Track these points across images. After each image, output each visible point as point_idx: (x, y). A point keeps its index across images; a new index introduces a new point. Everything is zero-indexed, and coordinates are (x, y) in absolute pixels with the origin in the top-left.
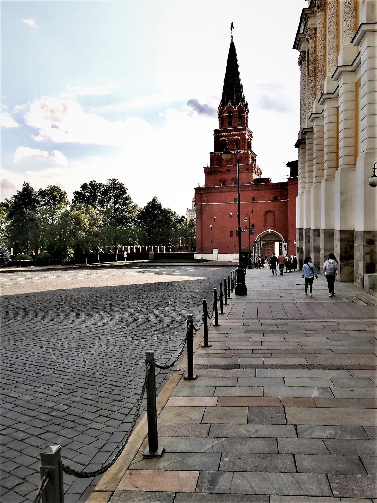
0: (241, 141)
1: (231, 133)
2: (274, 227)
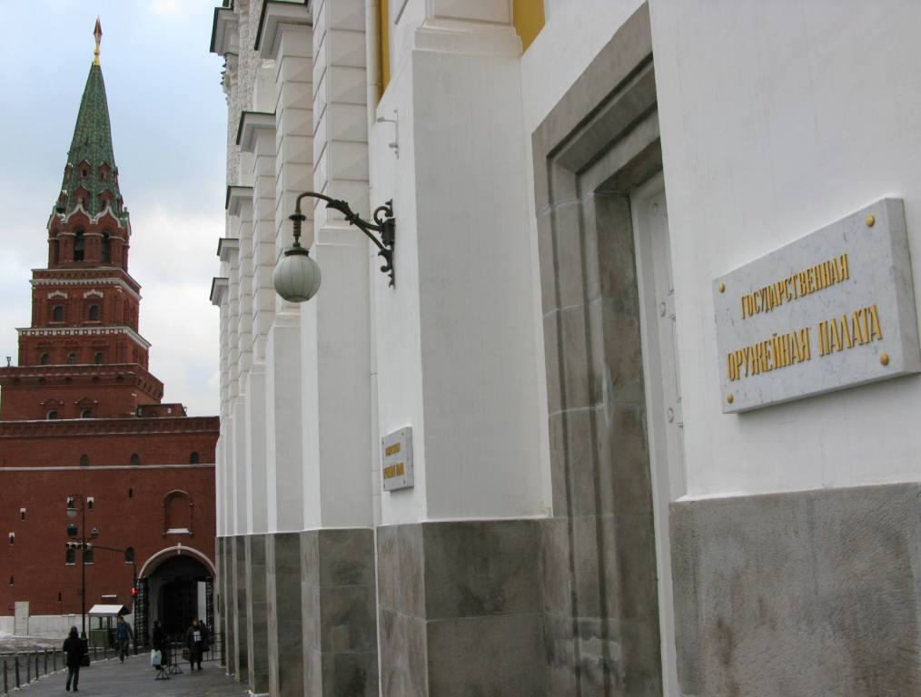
1: (81, 281)
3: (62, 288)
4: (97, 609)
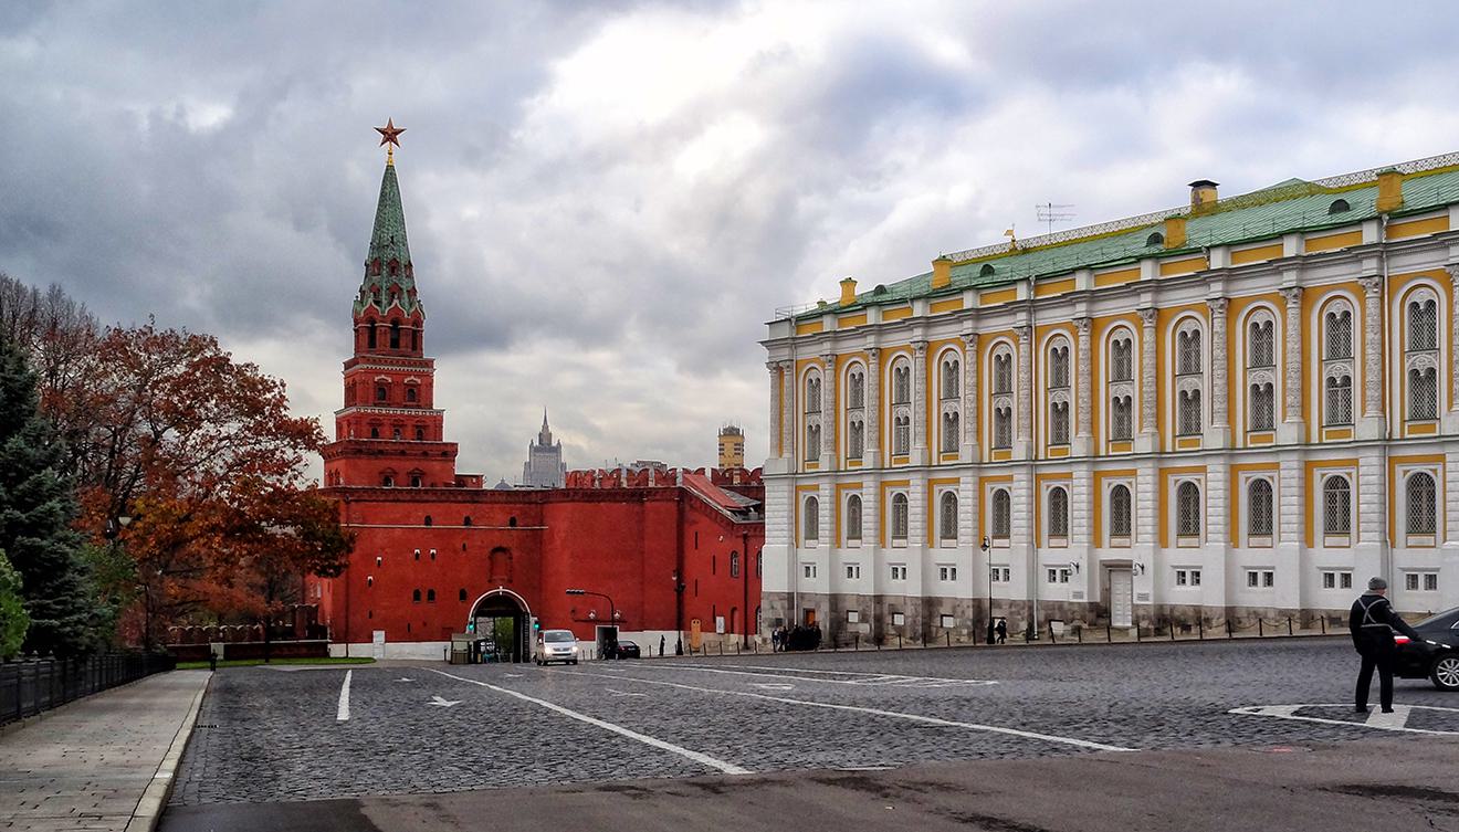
0: (423, 388)
2: (509, 583)
3: (387, 373)
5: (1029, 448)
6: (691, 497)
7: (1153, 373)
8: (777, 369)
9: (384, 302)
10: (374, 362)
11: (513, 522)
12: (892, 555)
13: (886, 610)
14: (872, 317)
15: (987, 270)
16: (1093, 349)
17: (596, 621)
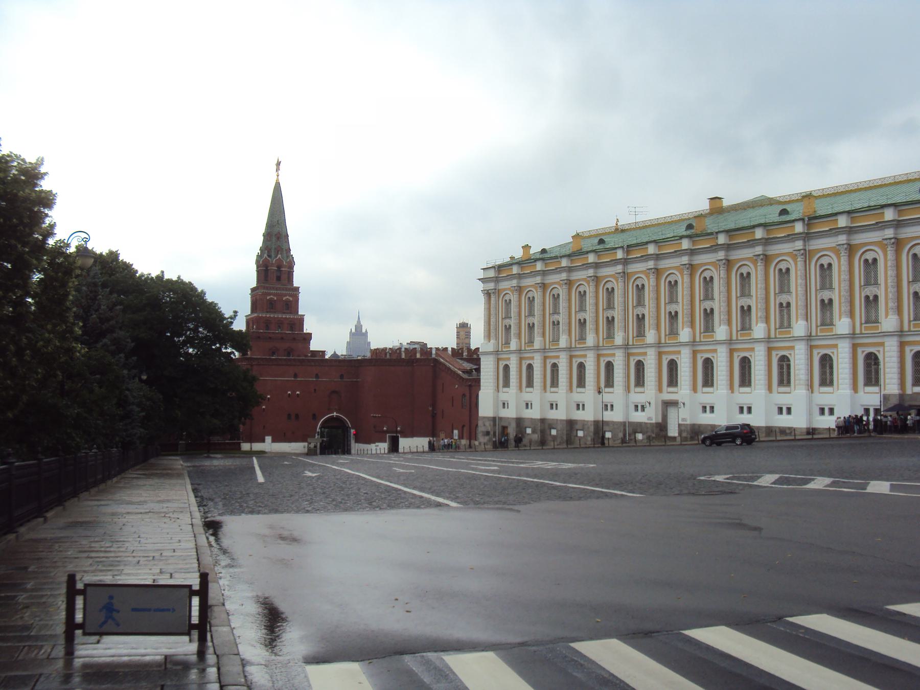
3: (274, 295)
4: (309, 440)
5: (624, 339)
6: (441, 363)
7: (689, 298)
8: (488, 294)
9: (273, 255)
10: (267, 288)
11: (342, 377)
12: (551, 397)
13: (547, 427)
14: (539, 266)
15: (601, 241)
16: (658, 285)
17: (387, 432)
